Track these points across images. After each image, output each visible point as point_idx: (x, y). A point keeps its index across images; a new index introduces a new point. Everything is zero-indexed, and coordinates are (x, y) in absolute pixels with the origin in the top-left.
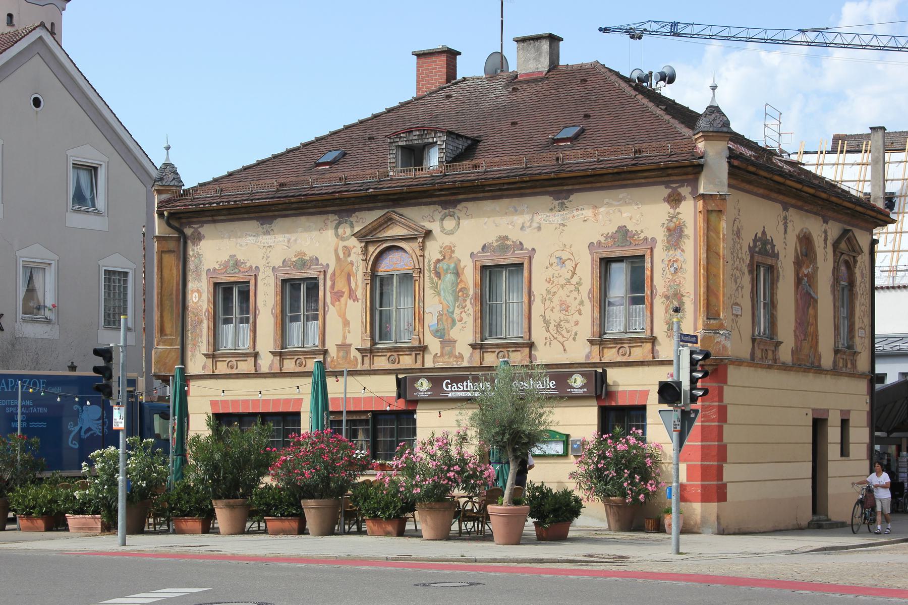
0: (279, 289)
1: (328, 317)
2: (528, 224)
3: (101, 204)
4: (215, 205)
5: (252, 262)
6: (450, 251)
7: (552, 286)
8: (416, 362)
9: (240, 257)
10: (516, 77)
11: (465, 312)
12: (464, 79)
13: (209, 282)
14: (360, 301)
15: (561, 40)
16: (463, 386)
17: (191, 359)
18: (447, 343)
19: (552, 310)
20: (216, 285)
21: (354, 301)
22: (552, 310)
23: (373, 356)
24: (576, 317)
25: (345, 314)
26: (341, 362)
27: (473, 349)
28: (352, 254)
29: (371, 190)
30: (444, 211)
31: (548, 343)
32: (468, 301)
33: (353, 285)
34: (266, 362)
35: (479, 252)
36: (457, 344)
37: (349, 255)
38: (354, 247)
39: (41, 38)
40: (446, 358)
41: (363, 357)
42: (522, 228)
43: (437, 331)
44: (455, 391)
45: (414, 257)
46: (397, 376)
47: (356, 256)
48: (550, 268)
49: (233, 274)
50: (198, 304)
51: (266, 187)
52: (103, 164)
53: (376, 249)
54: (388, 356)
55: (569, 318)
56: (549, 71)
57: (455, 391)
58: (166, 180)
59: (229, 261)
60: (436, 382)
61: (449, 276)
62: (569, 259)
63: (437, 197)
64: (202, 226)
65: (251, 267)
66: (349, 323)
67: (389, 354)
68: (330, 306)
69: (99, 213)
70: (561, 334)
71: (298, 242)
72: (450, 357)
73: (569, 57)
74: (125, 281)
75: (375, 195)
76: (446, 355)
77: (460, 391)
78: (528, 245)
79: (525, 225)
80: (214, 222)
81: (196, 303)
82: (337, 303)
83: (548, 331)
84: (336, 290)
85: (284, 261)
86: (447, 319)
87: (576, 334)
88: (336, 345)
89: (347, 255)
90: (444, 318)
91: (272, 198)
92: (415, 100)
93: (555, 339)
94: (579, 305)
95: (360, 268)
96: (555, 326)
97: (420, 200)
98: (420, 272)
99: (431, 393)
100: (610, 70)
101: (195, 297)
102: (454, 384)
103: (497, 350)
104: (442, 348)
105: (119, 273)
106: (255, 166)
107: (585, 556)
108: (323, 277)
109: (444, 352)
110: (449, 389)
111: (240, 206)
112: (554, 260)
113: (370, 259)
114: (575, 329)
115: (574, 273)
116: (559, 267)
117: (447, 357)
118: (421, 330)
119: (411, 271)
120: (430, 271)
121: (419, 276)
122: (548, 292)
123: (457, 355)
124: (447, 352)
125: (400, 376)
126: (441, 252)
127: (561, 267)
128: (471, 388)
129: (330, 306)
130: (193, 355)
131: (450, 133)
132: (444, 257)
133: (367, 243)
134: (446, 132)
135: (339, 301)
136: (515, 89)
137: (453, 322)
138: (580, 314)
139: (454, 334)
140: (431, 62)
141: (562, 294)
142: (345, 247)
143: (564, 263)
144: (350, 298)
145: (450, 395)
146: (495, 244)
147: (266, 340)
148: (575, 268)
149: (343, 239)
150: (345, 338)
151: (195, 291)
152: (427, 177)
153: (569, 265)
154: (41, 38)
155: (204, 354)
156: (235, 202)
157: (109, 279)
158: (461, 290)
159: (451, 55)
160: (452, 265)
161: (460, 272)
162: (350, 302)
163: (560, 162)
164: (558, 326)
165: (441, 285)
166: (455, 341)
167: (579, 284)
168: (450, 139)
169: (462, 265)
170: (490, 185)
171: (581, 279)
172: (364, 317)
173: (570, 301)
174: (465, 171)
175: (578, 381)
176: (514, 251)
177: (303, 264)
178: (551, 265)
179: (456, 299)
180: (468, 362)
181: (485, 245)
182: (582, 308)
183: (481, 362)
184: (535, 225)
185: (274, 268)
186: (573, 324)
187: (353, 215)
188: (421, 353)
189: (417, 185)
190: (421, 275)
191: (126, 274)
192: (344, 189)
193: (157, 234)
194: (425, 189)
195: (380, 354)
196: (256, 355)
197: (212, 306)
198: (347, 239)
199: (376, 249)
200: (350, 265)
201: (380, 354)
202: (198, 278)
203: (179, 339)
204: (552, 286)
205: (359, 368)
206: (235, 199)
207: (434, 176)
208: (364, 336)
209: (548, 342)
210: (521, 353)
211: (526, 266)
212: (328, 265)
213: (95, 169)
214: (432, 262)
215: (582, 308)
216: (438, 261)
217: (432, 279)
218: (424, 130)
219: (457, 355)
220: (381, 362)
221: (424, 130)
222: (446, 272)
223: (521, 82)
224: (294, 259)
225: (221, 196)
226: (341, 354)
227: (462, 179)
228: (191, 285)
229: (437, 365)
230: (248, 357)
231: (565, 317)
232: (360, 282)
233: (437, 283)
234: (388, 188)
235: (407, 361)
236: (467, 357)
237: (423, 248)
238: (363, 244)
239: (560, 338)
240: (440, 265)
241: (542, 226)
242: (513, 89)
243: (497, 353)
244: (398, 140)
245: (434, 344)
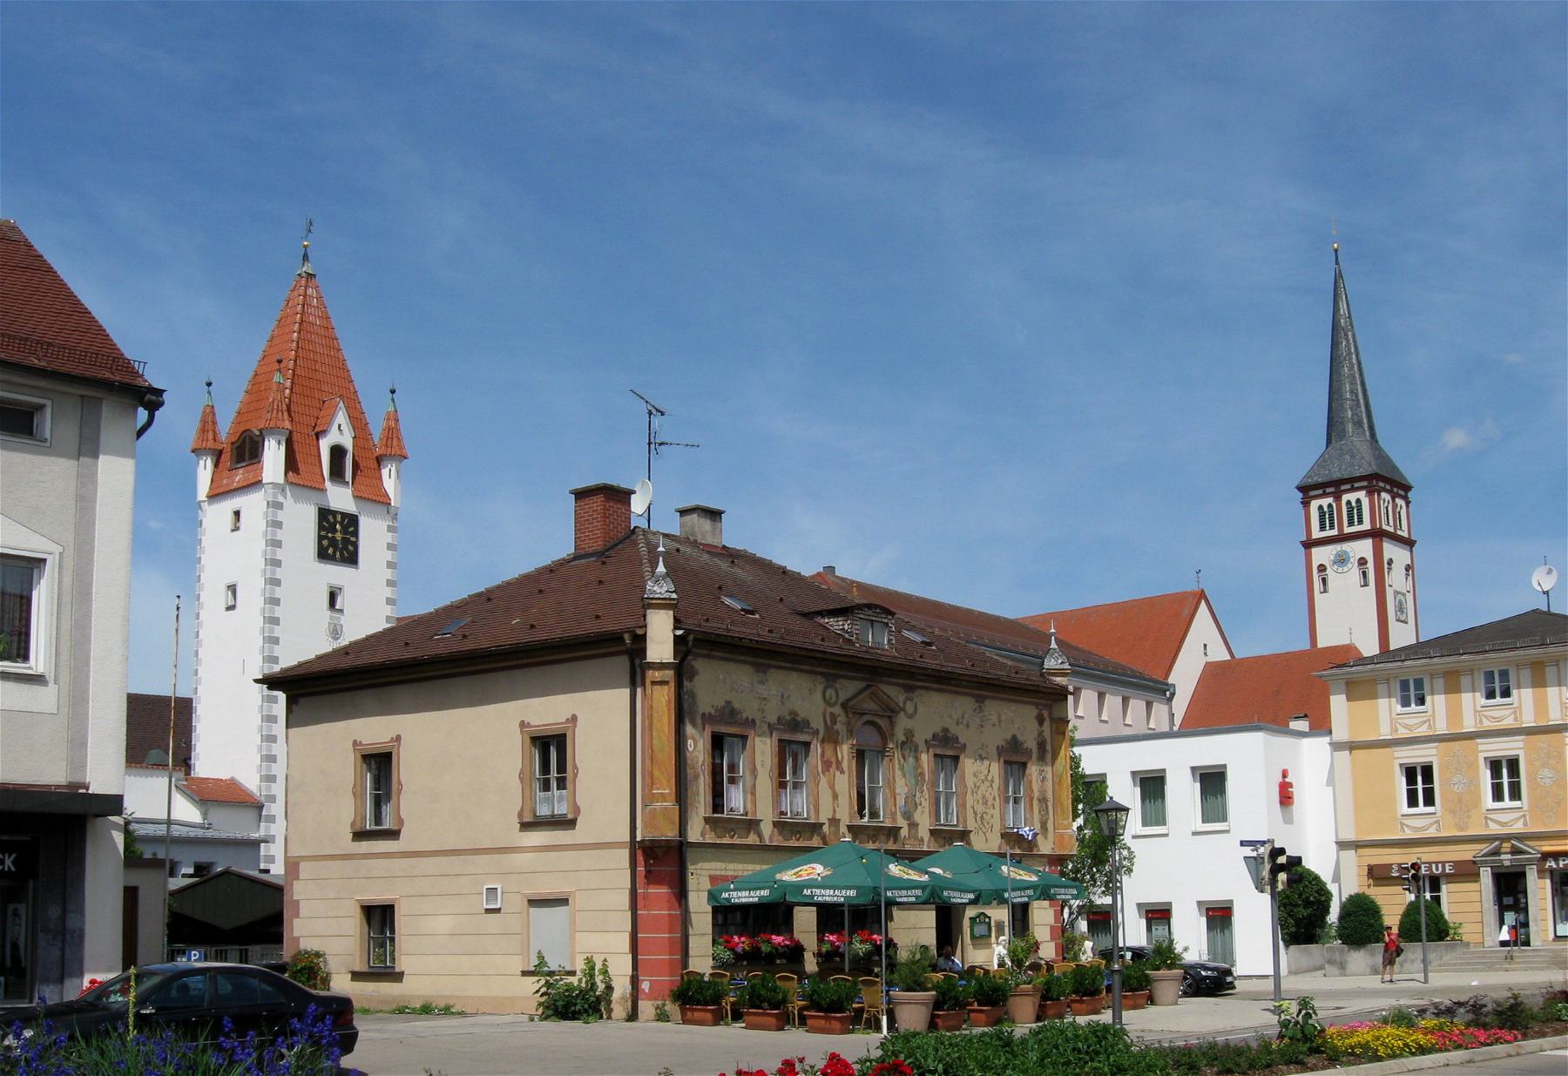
9: (736, 705)
28: (838, 723)
30: (906, 695)
33: (840, 756)
37: (835, 724)
38: (839, 715)
40: (912, 841)
65: (747, 718)
68: (821, 775)
84: (825, 759)
122: (975, 785)
126: (905, 734)
142: (831, 713)
162: (838, 773)
164: (982, 818)
167: (992, 781)
173: (987, 795)
179: (917, 784)
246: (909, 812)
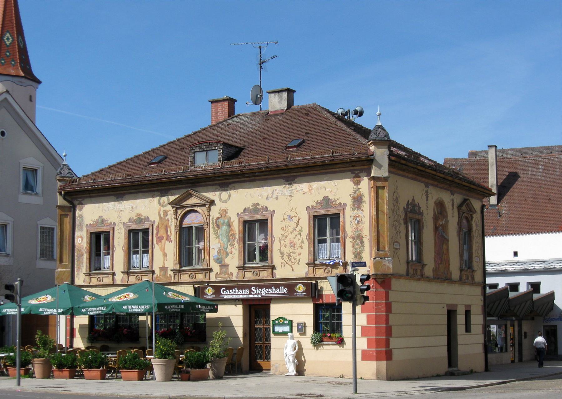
0: (127, 235)
1: (154, 251)
2: (271, 196)
3: (39, 188)
4: (90, 187)
5: (111, 220)
6: (225, 212)
7: (285, 232)
8: (205, 277)
9: (105, 217)
10: (268, 113)
11: (234, 248)
12: (239, 115)
13: (87, 231)
14: (173, 242)
15: (295, 91)
16: (233, 292)
17: (77, 277)
18: (224, 266)
19: (285, 246)
20: (91, 233)
21: (169, 242)
22: (285, 246)
23: (181, 274)
24: (300, 250)
25: (164, 249)
26: (162, 278)
27: (239, 269)
28: (168, 215)
29: (178, 178)
31: (283, 266)
32: (236, 241)
33: (169, 233)
34: (120, 277)
35: (242, 213)
36: (229, 267)
37: (167, 215)
38: (169, 210)
39: (6, 99)
40: (223, 275)
41: (175, 275)
42: (267, 198)
43: (218, 259)
44: (228, 295)
45: (204, 216)
46: (194, 286)
47: (171, 216)
48: (284, 222)
49: (101, 227)
50: (81, 245)
51: (119, 178)
52: (41, 167)
53: (182, 212)
54: (189, 274)
55: (295, 251)
56: (287, 109)
57: (228, 295)
58: (63, 174)
59: (98, 219)
60: (217, 290)
61: (224, 226)
62: (295, 216)
63: (217, 181)
64: (84, 200)
65: (111, 223)
66: (167, 255)
67: (189, 273)
68: (156, 245)
69: (37, 194)
70: (291, 261)
71: (137, 208)
72: (225, 274)
73: (299, 101)
74: (53, 233)
75: (181, 181)
76: (223, 273)
77: (248, 294)
78: (270, 208)
79: (269, 197)
80: (91, 197)
81: (80, 244)
82: (160, 243)
83: (283, 259)
85: (130, 219)
86: (223, 252)
87: (299, 260)
88: (159, 268)
89: (165, 215)
90: (222, 251)
91: (122, 183)
92: (210, 127)
93: (287, 263)
94: (301, 243)
95: (173, 223)
96: (287, 256)
97: (207, 183)
98: (208, 225)
99: (214, 296)
100: (323, 108)
101: (80, 241)
102: (228, 290)
103: (253, 270)
104: (221, 269)
105: (49, 228)
106: (116, 165)
107: (297, 395)
108: (152, 228)
109: (222, 271)
110: (225, 294)
111: (104, 188)
112: (286, 217)
113: (178, 217)
114: (299, 257)
115: (298, 225)
116: (289, 221)
117: (223, 274)
118: (208, 258)
119: (202, 224)
120: (213, 224)
121: (207, 227)
122: (283, 236)
123: (230, 273)
124: (223, 272)
125: (196, 286)
126: (219, 213)
127: (290, 221)
128: (237, 293)
129: (156, 245)
130: (78, 274)
131: (225, 144)
132: (222, 216)
133: (177, 209)
134: (223, 144)
135: (161, 242)
136: (267, 120)
137: (227, 254)
138: (302, 249)
139: (227, 261)
140: (219, 106)
141: (291, 237)
142: (164, 210)
143: (292, 218)
144: (167, 241)
145: (225, 297)
146: (251, 208)
147: (119, 266)
148: (298, 222)
149: (163, 206)
150: (164, 263)
151: (80, 237)
152: (211, 169)
153: (295, 220)
154: (6, 99)
155: (84, 274)
156: (101, 185)
157: (43, 232)
158: (231, 235)
159: (232, 102)
160: (226, 221)
161: (231, 224)
162: (167, 243)
163: (289, 159)
164: (289, 256)
165: (220, 232)
166: (228, 265)
167: (301, 231)
168: (225, 147)
169: (232, 220)
170: (247, 174)
171: (302, 228)
172: (175, 251)
173: (296, 241)
174: (233, 165)
175: (300, 289)
176: (262, 212)
177: (140, 220)
178: (284, 220)
179: (229, 241)
180: (236, 278)
181: (245, 208)
182: (303, 245)
183: (243, 278)
184: (274, 196)
185: (124, 224)
186: (298, 255)
187: (169, 192)
188: (208, 272)
189: (205, 174)
190: (208, 226)
191: (53, 229)
192: (163, 177)
193: (58, 205)
194: (210, 176)
195: (185, 273)
196: (114, 274)
197: (89, 245)
198: (166, 206)
199: (182, 212)
200: (167, 222)
201: (185, 273)
202: (81, 229)
203: (70, 265)
204: (285, 232)
205: (172, 281)
206: (101, 184)
207: (215, 169)
208: (175, 262)
209: (283, 265)
210: (267, 272)
211: (269, 221)
212: (154, 221)
213: (36, 170)
214: (214, 219)
215: (303, 245)
216: (218, 218)
217: (215, 229)
218: (210, 142)
219: (230, 273)
220: (185, 278)
221: (210, 142)
222: (223, 224)
223: (271, 115)
224: (135, 218)
225: (94, 182)
226: (162, 273)
227: (231, 170)
228: (77, 234)
229: (218, 280)
230: (109, 275)
231: (293, 250)
232: (173, 232)
233: (217, 231)
234: (188, 176)
235: (200, 277)
236: (235, 274)
237: (209, 210)
238: (175, 209)
239: (290, 263)
240: (219, 220)
241: (279, 197)
242: (266, 119)
243: (252, 272)
244: (195, 148)
245: (216, 267)
246: (222, 258)
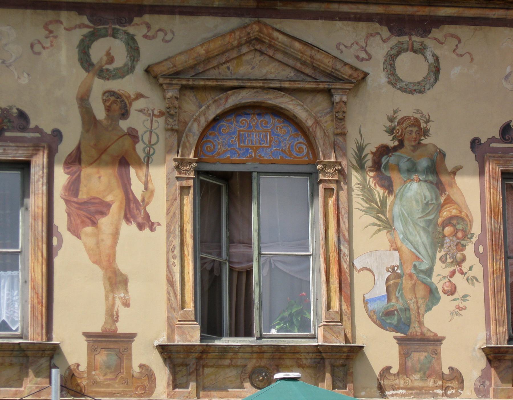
11: (462, 273)
32: (469, 251)
35: (493, 140)
36: (444, 347)
43: (388, 314)
76: (415, 371)
86: (414, 286)
90: (407, 284)
104: (404, 356)
109: (409, 364)
117: (417, 376)
123: (446, 371)
124: (419, 366)
126: (391, 131)
158: (448, 222)
166: (438, 341)
217: (370, 190)
219: (446, 371)
233: (384, 203)
